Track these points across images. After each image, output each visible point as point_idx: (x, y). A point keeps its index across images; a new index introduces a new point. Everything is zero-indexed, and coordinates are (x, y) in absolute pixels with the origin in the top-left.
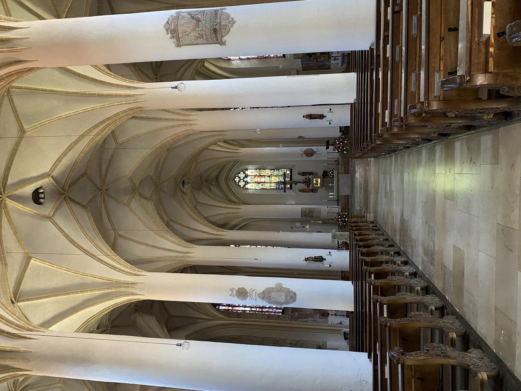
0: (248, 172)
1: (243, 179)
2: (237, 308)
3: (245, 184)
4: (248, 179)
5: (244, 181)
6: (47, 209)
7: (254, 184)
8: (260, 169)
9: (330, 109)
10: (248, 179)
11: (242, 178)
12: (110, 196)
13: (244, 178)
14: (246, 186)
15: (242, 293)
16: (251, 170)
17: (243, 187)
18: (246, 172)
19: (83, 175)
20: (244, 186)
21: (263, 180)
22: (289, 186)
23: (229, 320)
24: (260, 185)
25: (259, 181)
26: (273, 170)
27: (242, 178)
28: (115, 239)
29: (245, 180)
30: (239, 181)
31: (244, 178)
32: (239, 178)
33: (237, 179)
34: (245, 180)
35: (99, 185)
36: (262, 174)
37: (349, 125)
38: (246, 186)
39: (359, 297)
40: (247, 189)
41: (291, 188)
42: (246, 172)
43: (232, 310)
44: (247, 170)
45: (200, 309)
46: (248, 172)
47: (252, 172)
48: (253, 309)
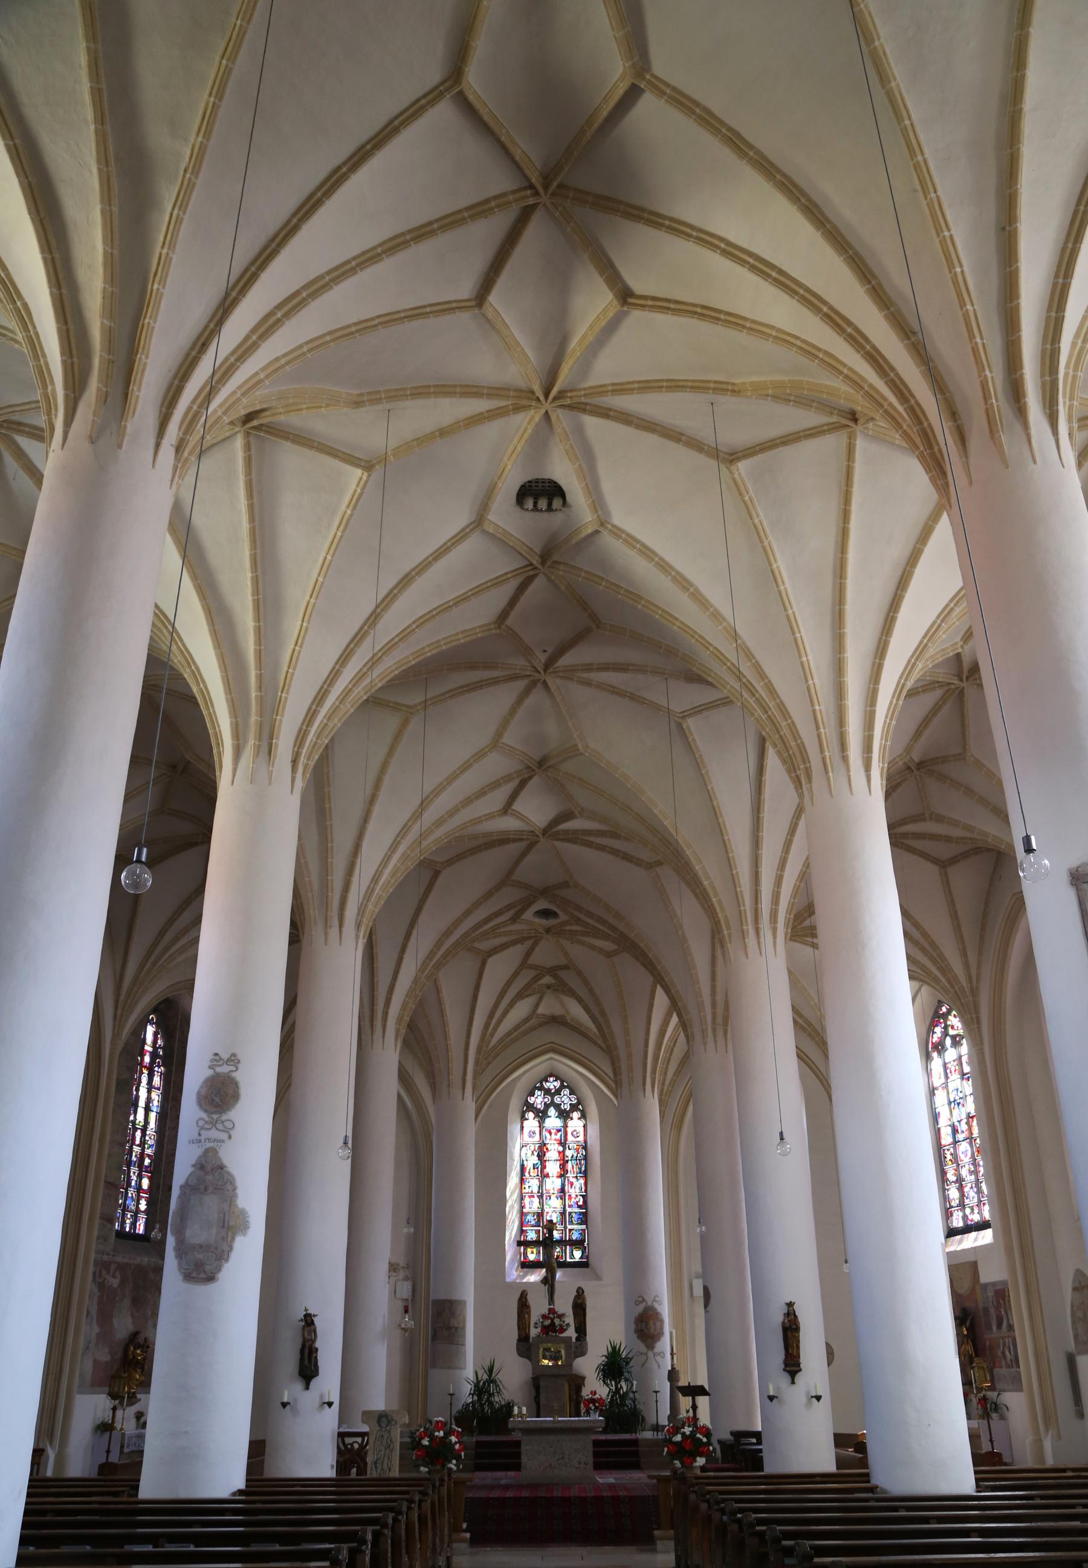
0: (576, 1123)
1: (553, 1104)
4: (553, 1121)
6: (504, 515)
7: (537, 1138)
8: (585, 1158)
9: (818, 1398)
10: (553, 1121)
11: (557, 1100)
12: (527, 691)
13: (557, 1107)
16: (581, 1130)
17: (527, 1103)
19: (594, 617)
20: (531, 1107)
21: (553, 1168)
22: (532, 1257)
23: (111, 1055)
24: (535, 1159)
25: (548, 1155)
26: (585, 1202)
27: (557, 1100)
28: (395, 707)
29: (552, 1112)
30: (548, 1092)
31: (557, 1107)
32: (558, 1092)
33: (552, 1084)
34: (552, 1112)
36: (569, 1166)
37: (769, 1468)
38: (531, 1115)
39: (190, 1514)
40: (523, 1118)
42: (576, 1115)
44: (583, 1116)
45: (155, 963)
46: (576, 1123)
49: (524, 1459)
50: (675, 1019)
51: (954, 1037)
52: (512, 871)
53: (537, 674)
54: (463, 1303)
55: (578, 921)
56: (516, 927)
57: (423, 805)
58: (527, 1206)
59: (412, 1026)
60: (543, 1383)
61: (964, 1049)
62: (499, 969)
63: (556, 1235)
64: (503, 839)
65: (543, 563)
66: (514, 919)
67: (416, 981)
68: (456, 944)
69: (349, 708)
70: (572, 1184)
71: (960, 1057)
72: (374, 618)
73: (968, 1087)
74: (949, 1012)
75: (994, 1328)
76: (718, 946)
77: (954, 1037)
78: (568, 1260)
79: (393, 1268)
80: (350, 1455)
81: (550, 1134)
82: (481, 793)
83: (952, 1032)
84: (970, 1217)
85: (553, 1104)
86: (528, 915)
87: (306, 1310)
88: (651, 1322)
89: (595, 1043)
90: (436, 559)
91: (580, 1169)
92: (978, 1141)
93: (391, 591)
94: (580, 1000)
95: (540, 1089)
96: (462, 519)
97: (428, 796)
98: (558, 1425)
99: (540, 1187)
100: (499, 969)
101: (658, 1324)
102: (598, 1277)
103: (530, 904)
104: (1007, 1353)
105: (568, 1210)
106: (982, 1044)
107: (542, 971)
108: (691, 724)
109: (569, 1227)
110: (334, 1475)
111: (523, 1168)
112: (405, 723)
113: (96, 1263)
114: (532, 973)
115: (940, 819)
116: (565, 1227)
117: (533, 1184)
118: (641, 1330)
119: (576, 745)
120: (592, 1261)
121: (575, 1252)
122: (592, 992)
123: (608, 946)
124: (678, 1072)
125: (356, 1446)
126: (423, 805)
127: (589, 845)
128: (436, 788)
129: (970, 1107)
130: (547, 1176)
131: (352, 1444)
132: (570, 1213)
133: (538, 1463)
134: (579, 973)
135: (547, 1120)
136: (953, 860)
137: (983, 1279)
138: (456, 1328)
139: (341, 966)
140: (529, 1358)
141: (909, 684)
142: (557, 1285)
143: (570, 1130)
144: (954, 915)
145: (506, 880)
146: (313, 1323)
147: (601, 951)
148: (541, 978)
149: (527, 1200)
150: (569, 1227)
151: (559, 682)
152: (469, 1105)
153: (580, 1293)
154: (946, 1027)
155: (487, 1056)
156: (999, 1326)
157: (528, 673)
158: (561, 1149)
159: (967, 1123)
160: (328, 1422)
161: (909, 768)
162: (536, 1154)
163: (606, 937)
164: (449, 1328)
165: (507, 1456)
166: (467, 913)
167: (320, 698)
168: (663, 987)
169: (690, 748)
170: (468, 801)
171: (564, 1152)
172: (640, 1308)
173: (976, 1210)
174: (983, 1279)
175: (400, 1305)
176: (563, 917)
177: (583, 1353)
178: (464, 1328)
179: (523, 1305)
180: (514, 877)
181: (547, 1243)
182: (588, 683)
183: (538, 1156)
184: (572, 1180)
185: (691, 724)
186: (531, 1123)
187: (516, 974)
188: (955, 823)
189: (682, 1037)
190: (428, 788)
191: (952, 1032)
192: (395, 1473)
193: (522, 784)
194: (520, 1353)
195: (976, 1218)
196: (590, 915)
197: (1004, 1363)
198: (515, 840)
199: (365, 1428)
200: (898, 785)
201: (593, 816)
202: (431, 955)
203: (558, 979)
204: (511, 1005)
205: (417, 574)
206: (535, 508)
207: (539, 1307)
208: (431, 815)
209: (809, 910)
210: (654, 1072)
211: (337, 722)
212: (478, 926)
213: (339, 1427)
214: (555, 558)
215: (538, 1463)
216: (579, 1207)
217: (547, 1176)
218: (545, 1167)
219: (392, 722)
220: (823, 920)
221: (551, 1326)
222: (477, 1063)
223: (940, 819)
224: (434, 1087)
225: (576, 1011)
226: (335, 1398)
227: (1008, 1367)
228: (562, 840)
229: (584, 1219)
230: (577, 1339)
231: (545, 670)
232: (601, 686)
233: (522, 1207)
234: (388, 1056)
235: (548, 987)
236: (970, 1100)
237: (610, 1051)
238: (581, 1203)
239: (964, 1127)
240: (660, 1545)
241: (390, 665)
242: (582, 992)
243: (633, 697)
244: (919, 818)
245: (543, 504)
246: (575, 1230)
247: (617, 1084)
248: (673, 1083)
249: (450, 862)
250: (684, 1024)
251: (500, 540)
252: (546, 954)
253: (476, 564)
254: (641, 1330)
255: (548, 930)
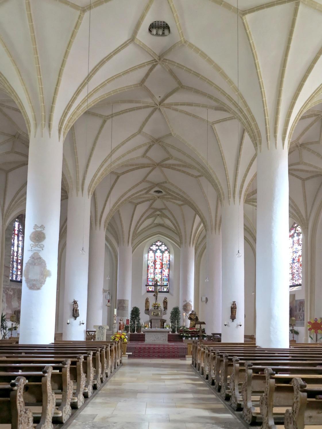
1: (159, 249)
2: (16, 237)
3: (153, 251)
4: (159, 254)
5: (157, 250)
7: (153, 258)
10: (159, 254)
13: (160, 250)
14: (151, 252)
15: (39, 237)
17: (150, 249)
18: (167, 252)
20: (151, 250)
21: (158, 266)
22: (150, 290)
25: (156, 263)
26: (169, 276)
27: (160, 248)
29: (158, 251)
30: (157, 245)
34: (158, 251)
35: (166, 102)
36: (164, 266)
38: (151, 252)
41: (148, 291)
43: (14, 233)
47: (166, 257)
48: (15, 254)
49: (146, 338)
50: (202, 225)
51: (298, 233)
52: (146, 177)
53: (156, 106)
54: (128, 301)
55: (169, 194)
56: (147, 196)
57: (113, 152)
58: (149, 276)
59: (110, 224)
60: (153, 321)
61: (301, 237)
62: (141, 209)
63: (158, 284)
64: (143, 166)
65: (160, 59)
66: (147, 193)
67: (111, 210)
68: (125, 200)
69: (81, 112)
70: (164, 271)
71: (299, 239)
72: (89, 78)
73: (300, 248)
74: (297, 226)
75: (298, 311)
76: (219, 203)
77: (298, 233)
78: (162, 291)
79: (104, 291)
80: (90, 335)
81: (158, 257)
82: (134, 149)
83: (297, 232)
84: (295, 283)
85: (159, 249)
86: (152, 192)
87: (74, 300)
88: (188, 307)
89: (173, 231)
90: (114, 54)
91: (167, 267)
92: (301, 263)
93: (96, 67)
94: (169, 219)
95: (154, 245)
96: (125, 38)
97: (114, 149)
98: (157, 330)
99: (154, 271)
100: (141, 209)
101: (190, 307)
102: (172, 295)
103: (152, 188)
104: (301, 317)
105: (163, 278)
106: (308, 235)
107: (156, 210)
108: (216, 127)
109: (163, 282)
110: (85, 340)
111: (148, 266)
112: (105, 122)
113: (4, 288)
114: (153, 211)
115: (306, 164)
116: (162, 282)
117: (151, 270)
118: (185, 309)
119: (171, 133)
120: (170, 291)
121: (164, 289)
122: (173, 216)
123: (180, 203)
124: (202, 241)
125: (93, 334)
126: (113, 152)
127: (175, 169)
128: (117, 147)
129: (300, 253)
130: (156, 268)
131: (92, 334)
132: (163, 279)
133: (150, 340)
134: (169, 211)
135: (157, 253)
136: (308, 179)
137: (296, 298)
138: (125, 307)
139: (83, 206)
140: (149, 315)
141: (301, 115)
142: (158, 297)
143: (164, 256)
144: (305, 197)
145: (144, 180)
146: (77, 303)
147: (177, 204)
148: (156, 212)
149: (149, 275)
150: (163, 282)
151: (165, 109)
152: (130, 248)
153: (166, 299)
154: (296, 230)
155: (136, 235)
156: (300, 310)
157: (153, 105)
158: (161, 261)
159: (298, 258)
160: (84, 328)
161: (297, 146)
162: (153, 262)
163: (179, 200)
164: (124, 307)
165: (141, 338)
166: (130, 190)
167: (69, 107)
168: (198, 215)
169: (215, 135)
170: (129, 152)
171: (162, 262)
172: (185, 303)
173: (297, 281)
174: (296, 298)
175: (107, 301)
176: (164, 193)
177: (166, 314)
178: (128, 307)
179: (147, 301)
180: (146, 179)
181: (156, 285)
182: (176, 110)
183: (153, 263)
184: (164, 270)
185: (216, 127)
186: (151, 254)
187: (147, 211)
188: (311, 165)
189: (204, 230)
190: (113, 147)
191: (297, 232)
192: (105, 340)
193: (150, 147)
194: (146, 313)
195: (297, 283)
196: (174, 192)
197: (299, 320)
198: (147, 167)
199: (95, 330)
200: (292, 151)
201: (176, 159)
202: (116, 203)
203: (161, 212)
204: (145, 220)
205: (107, 60)
206: (157, 34)
207: (152, 302)
208: (114, 156)
209: (255, 192)
210: (194, 240)
211: (76, 118)
212: (134, 194)
213: (86, 329)
214: (165, 57)
215: (150, 340)
216: (166, 277)
217: (156, 268)
218: (155, 266)
219: (98, 122)
220: (259, 195)
221: (156, 307)
222: (133, 236)
223: (306, 164)
224: (118, 243)
225: (168, 222)
226: (85, 322)
227: (300, 320)
228: (165, 167)
229: (168, 280)
230: (164, 310)
231: (160, 105)
232: (181, 111)
233: (148, 276)
234: (102, 233)
235: (158, 215)
236: (300, 251)
237: (179, 234)
238: (167, 276)
239: (297, 259)
240: (187, 359)
241: (96, 96)
242: (170, 216)
243: (194, 116)
244: (298, 164)
245: (160, 32)
246: (165, 283)
247: (180, 244)
248: (200, 244)
249: (123, 173)
250: (205, 226)
251: (142, 48)
252: (158, 204)
253: (131, 57)
254: (185, 309)
255: (158, 197)
